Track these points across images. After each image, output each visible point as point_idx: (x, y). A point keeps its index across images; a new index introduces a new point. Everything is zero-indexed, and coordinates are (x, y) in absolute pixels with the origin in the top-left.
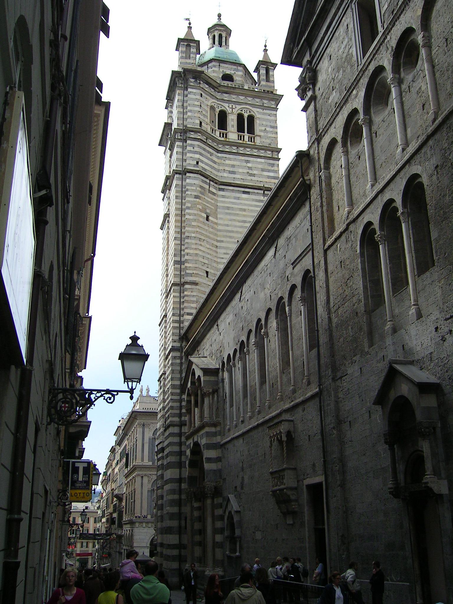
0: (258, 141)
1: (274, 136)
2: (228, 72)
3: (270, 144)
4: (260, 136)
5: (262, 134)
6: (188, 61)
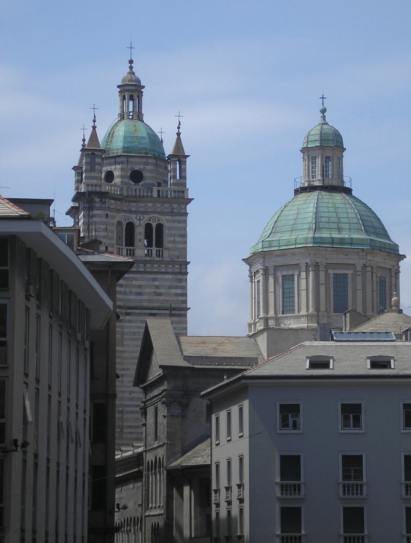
0: (166, 254)
1: (182, 246)
2: (137, 168)
3: (178, 257)
4: (168, 249)
5: (171, 245)
6: (93, 174)
